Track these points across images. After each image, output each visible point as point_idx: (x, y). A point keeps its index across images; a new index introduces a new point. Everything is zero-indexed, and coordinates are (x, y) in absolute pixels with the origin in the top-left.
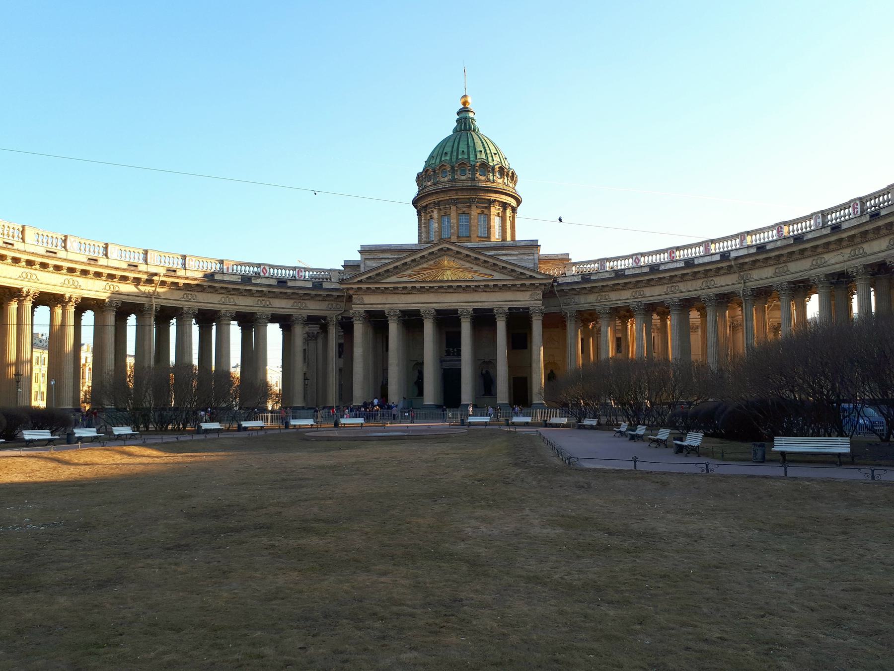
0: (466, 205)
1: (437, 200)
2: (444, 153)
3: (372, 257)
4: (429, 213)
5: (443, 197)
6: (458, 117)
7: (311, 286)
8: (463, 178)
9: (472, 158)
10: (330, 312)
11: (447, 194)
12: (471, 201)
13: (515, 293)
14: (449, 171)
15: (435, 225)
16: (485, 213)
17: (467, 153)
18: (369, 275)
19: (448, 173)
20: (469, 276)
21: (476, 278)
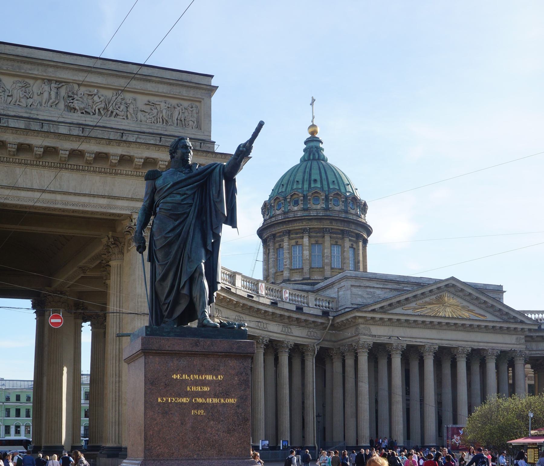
0: (338, 236)
1: (309, 227)
2: (312, 180)
3: (358, 285)
4: (293, 239)
5: (316, 225)
6: (305, 146)
7: (295, 310)
8: (337, 208)
9: (343, 190)
10: (309, 340)
11: (320, 222)
12: (343, 232)
13: (504, 336)
14: (323, 200)
15: (286, 254)
16: (354, 247)
17: (337, 184)
18: (383, 304)
19: (321, 202)
20: (466, 314)
21: (472, 317)
